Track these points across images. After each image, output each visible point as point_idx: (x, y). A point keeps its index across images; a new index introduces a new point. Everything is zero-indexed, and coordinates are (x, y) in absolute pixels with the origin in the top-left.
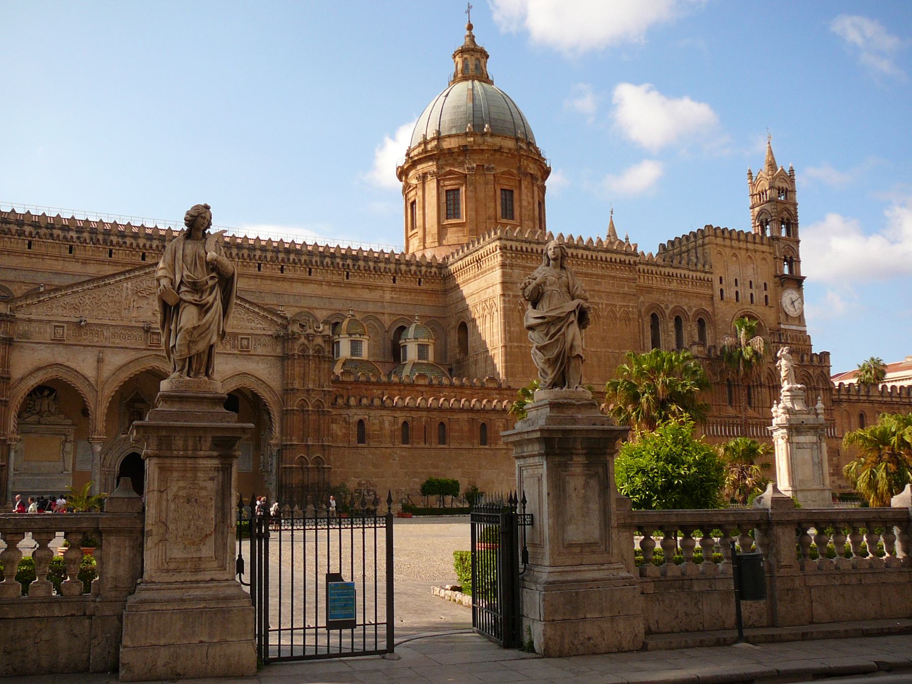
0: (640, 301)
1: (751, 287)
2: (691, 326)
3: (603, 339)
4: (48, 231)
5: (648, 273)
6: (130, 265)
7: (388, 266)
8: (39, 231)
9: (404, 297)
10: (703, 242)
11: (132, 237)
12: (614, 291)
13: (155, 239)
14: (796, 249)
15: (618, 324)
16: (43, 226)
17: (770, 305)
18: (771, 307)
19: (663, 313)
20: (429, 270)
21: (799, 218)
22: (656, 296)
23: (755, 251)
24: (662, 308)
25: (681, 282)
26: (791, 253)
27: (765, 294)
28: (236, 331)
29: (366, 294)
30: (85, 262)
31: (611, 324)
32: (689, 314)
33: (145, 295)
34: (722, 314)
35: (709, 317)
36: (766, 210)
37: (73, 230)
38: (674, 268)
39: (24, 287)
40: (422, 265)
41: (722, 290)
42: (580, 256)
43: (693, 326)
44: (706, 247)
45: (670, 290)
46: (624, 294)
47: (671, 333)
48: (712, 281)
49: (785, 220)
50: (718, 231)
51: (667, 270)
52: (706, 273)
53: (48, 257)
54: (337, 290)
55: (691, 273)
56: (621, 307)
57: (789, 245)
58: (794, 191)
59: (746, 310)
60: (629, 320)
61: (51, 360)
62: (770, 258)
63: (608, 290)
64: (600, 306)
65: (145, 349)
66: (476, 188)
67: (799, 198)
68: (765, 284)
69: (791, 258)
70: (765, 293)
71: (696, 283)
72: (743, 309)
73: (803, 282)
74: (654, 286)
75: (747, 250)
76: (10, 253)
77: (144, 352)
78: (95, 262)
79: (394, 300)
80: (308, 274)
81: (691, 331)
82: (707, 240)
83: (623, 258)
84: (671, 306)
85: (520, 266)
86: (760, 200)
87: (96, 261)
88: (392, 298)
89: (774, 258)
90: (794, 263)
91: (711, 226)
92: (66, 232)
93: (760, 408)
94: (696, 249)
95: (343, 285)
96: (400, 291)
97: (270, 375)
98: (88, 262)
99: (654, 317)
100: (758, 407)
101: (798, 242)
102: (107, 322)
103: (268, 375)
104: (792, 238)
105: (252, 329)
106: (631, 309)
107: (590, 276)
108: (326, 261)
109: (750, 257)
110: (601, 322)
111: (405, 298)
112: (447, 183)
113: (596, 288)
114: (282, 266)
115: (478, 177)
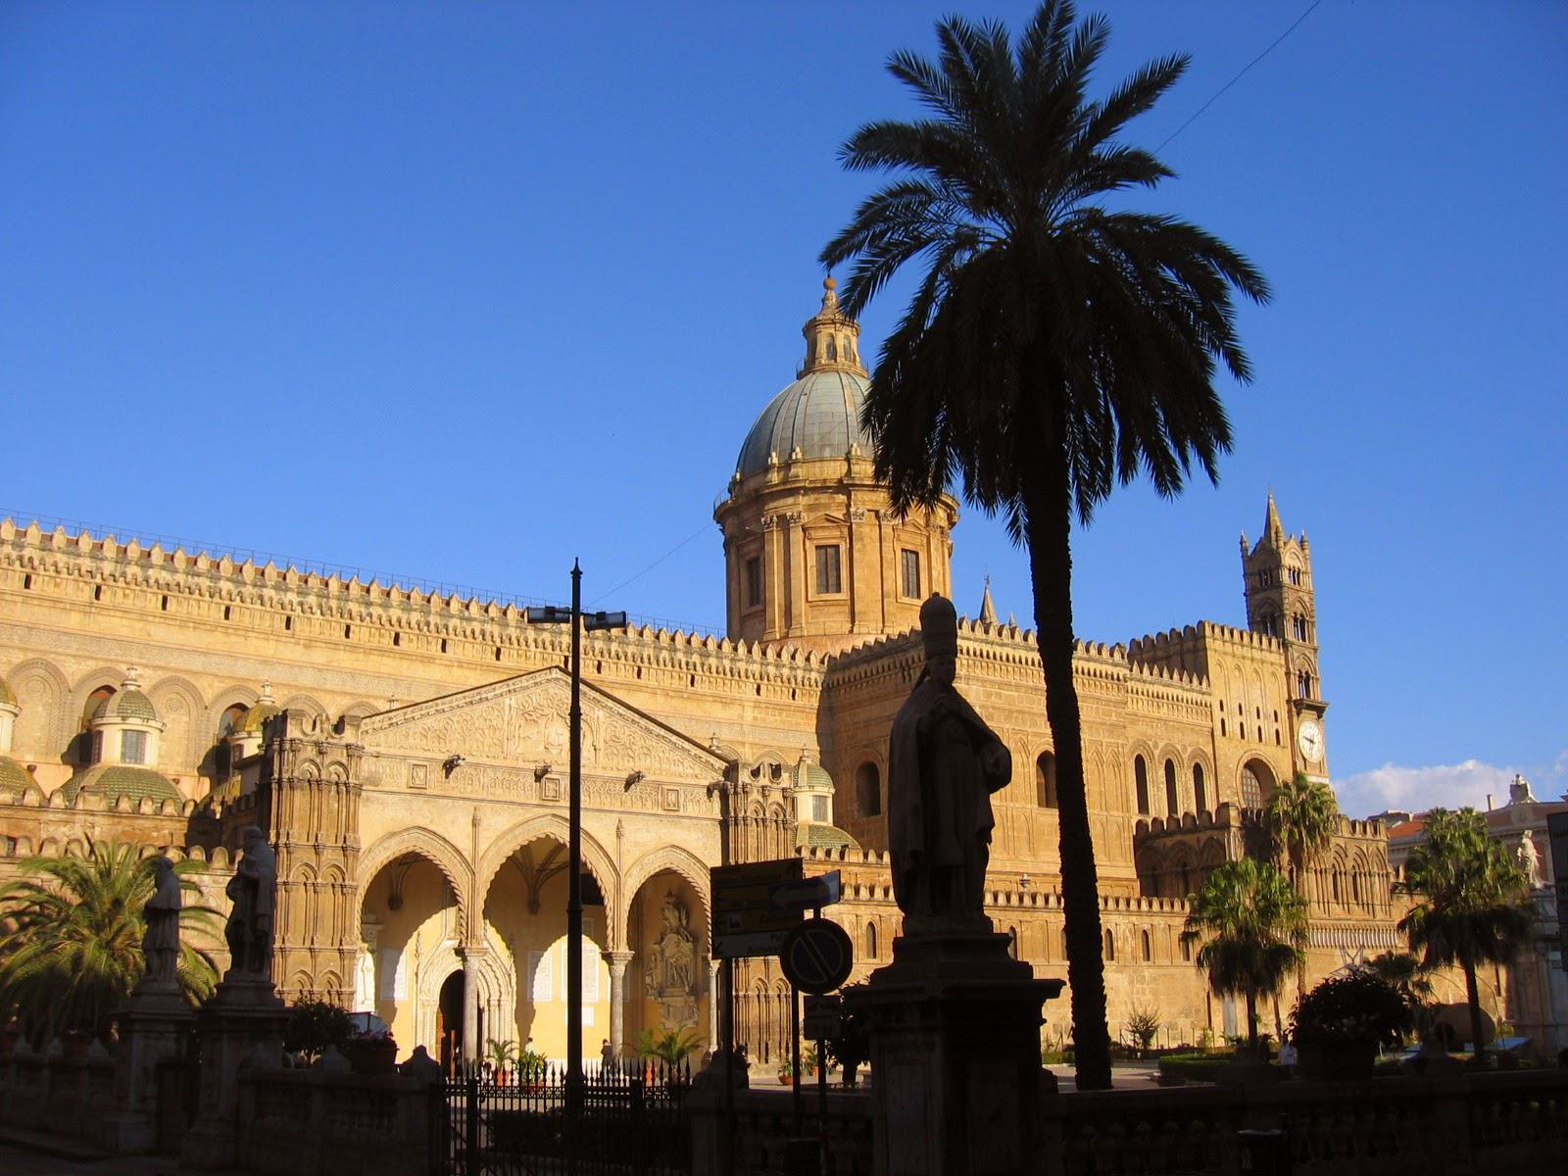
1: (1259, 717)
4: (255, 591)
5: (1158, 697)
6: (376, 652)
7: (750, 668)
8: (243, 590)
9: (772, 718)
10: (1195, 646)
11: (380, 605)
13: (415, 610)
16: (248, 582)
17: (1282, 744)
20: (807, 676)
22: (1141, 728)
24: (1149, 746)
28: (660, 778)
29: (718, 711)
30: (309, 644)
33: (535, 717)
37: (292, 590)
38: (1164, 685)
39: (216, 684)
40: (798, 667)
41: (1223, 721)
43: (1188, 775)
46: (1111, 725)
48: (1211, 705)
49: (1298, 616)
52: (1203, 694)
53: (254, 634)
54: (677, 703)
56: (1109, 745)
57: (1304, 654)
59: (1254, 752)
61: (409, 822)
63: (1091, 719)
65: (538, 806)
66: (864, 546)
69: (1307, 673)
70: (1276, 726)
72: (1251, 750)
74: (1140, 712)
75: (1252, 659)
76: (197, 625)
77: (537, 809)
78: (324, 645)
79: (758, 723)
80: (636, 676)
81: (1186, 783)
84: (1161, 745)
85: (977, 679)
87: (326, 643)
88: (755, 719)
92: (282, 594)
94: (1182, 654)
95: (685, 696)
96: (767, 708)
97: (706, 849)
98: (314, 643)
99: (1140, 762)
102: (485, 760)
103: (703, 849)
104: (1307, 642)
105: (680, 776)
108: (662, 655)
109: (1256, 672)
111: (774, 719)
112: (820, 534)
114: (600, 663)
115: (866, 530)
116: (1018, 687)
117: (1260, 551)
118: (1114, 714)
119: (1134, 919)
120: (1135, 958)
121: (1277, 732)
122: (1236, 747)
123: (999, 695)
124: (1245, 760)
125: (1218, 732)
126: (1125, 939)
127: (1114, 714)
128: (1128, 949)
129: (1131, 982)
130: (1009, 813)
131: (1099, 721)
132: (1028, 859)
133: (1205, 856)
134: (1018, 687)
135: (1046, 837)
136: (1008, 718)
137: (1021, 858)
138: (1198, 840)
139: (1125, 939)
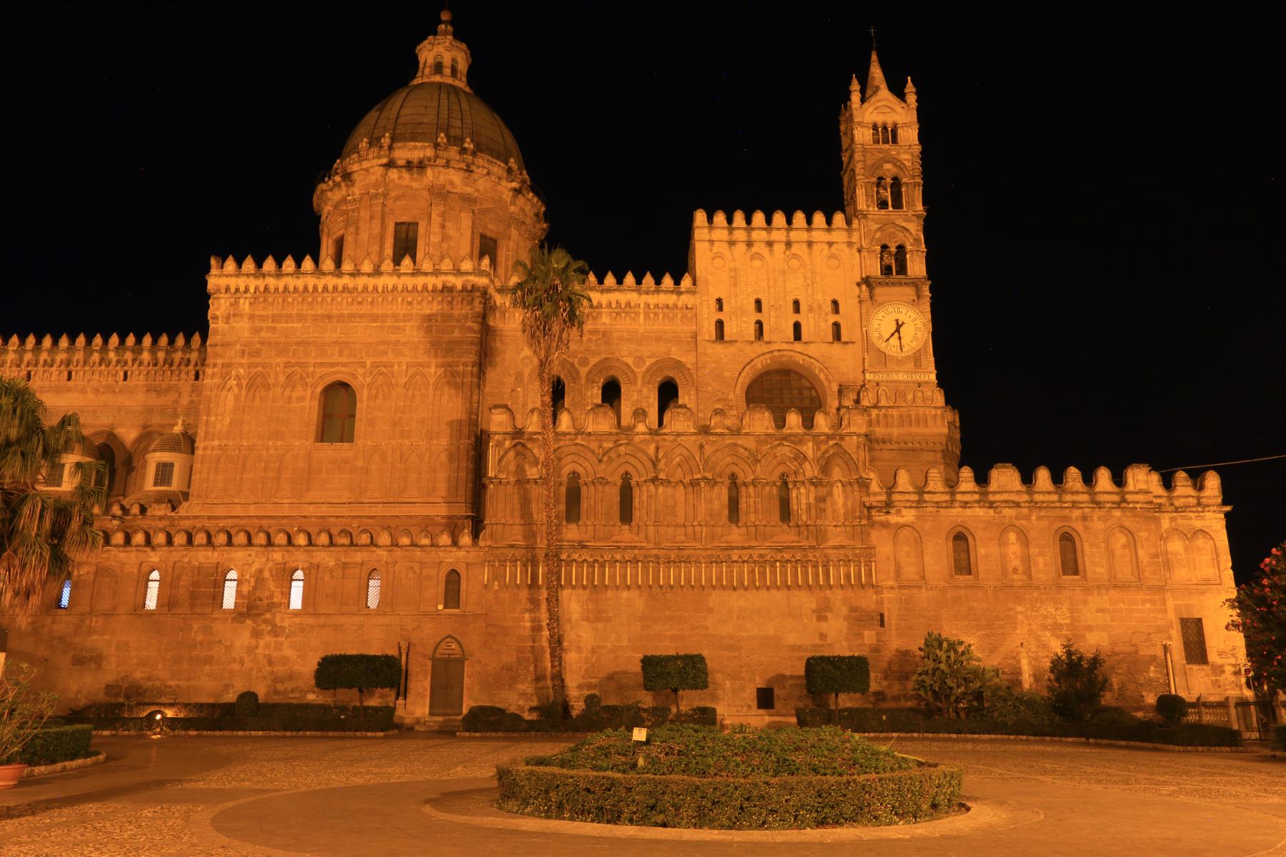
0: (521, 356)
18: (846, 343)
19: (575, 375)
27: (832, 321)
32: (635, 369)
34: (713, 365)
35: (686, 373)
43: (645, 391)
64: (396, 367)
66: (357, 229)
70: (833, 318)
71: (656, 314)
72: (772, 352)
84: (593, 361)
113: (393, 338)
118: (456, 331)
123: (273, 330)
129: (256, 634)
134: (301, 318)
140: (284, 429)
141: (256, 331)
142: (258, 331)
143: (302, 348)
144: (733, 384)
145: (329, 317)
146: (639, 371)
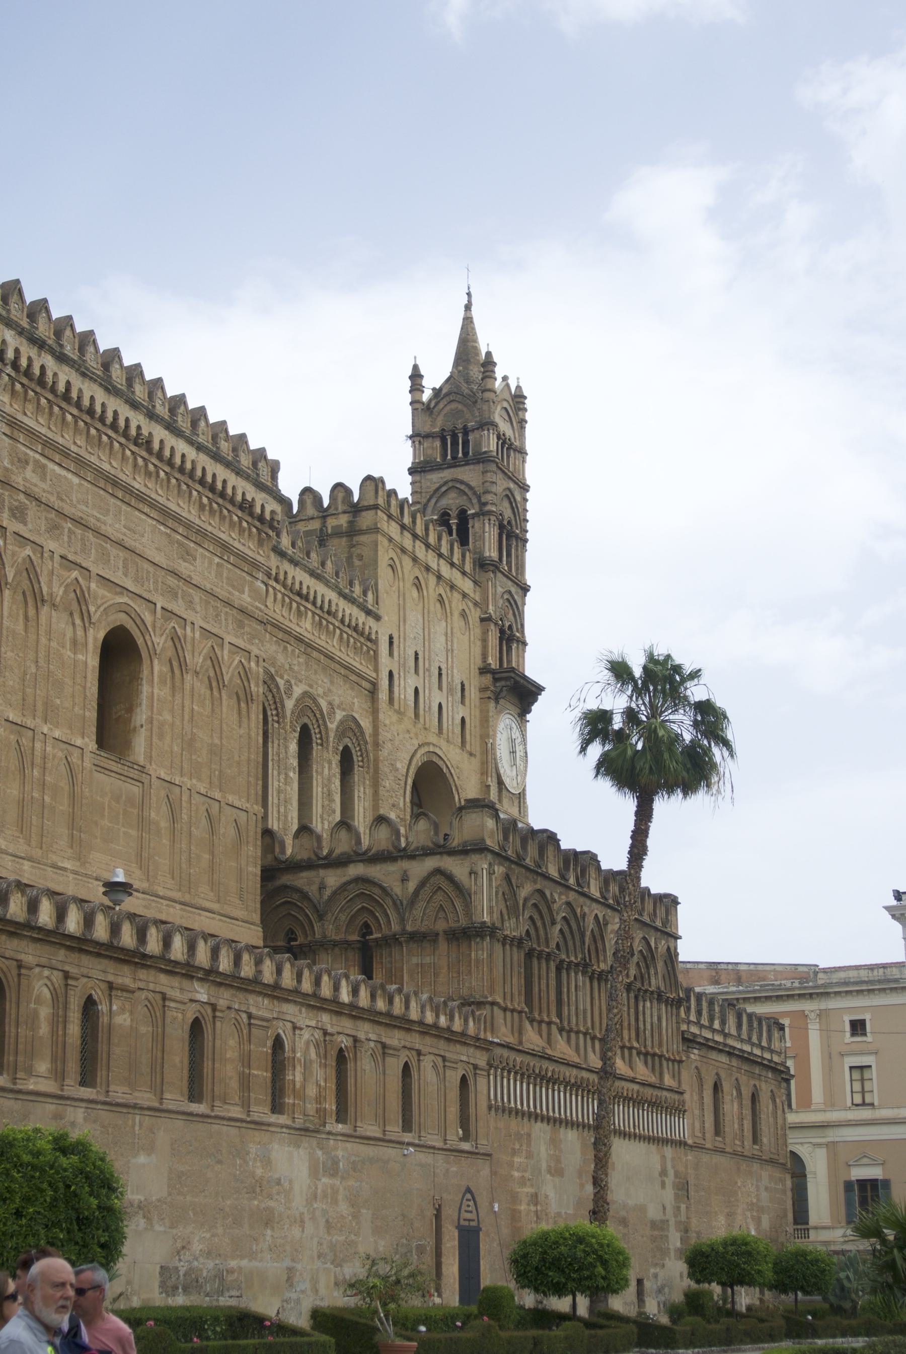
2: (330, 763)
3: (190, 744)
10: (351, 523)
12: (217, 591)
14: (519, 604)
15: (225, 703)
19: (279, 705)
21: (529, 526)
23: (453, 587)
25: (320, 623)
26: (511, 616)
31: (208, 702)
36: (462, 482)
38: (313, 574)
41: (391, 674)
42: (156, 446)
44: (363, 538)
45: (299, 639)
47: (291, 774)
48: (375, 642)
49: (505, 523)
50: (393, 502)
51: (299, 576)
52: (369, 613)
55: (343, 604)
57: (510, 592)
58: (522, 452)
60: (249, 698)
62: (475, 615)
63: (208, 587)
64: (188, 629)
67: (532, 472)
68: (463, 685)
69: (510, 627)
70: (461, 712)
72: (428, 744)
73: (536, 700)
75: (439, 577)
81: (329, 780)
82: (366, 519)
83: (252, 493)
84: (298, 691)
86: (444, 455)
89: (482, 620)
90: (514, 646)
91: (381, 480)
93: (581, 1036)
100: (578, 1032)
101: (525, 589)
106: (253, 664)
107: (170, 523)
109: (441, 600)
110: (187, 686)
113: (184, 568)
116: (80, 462)
117: (447, 395)
118: (247, 589)
119: (325, 1018)
120: (321, 1113)
121: (463, 720)
122: (408, 731)
124: (418, 761)
125: (383, 695)
126: (307, 1066)
127: (247, 589)
128: (312, 1091)
130: (38, 745)
131: (223, 594)
132: (67, 865)
133: (418, 912)
135: (105, 823)
136: (54, 528)
137: (54, 858)
138: (405, 879)
139: (307, 1066)
140: (58, 701)
141: (19, 460)
142: (24, 462)
143: (79, 531)
144: (402, 783)
145: (115, 482)
146: (332, 726)
